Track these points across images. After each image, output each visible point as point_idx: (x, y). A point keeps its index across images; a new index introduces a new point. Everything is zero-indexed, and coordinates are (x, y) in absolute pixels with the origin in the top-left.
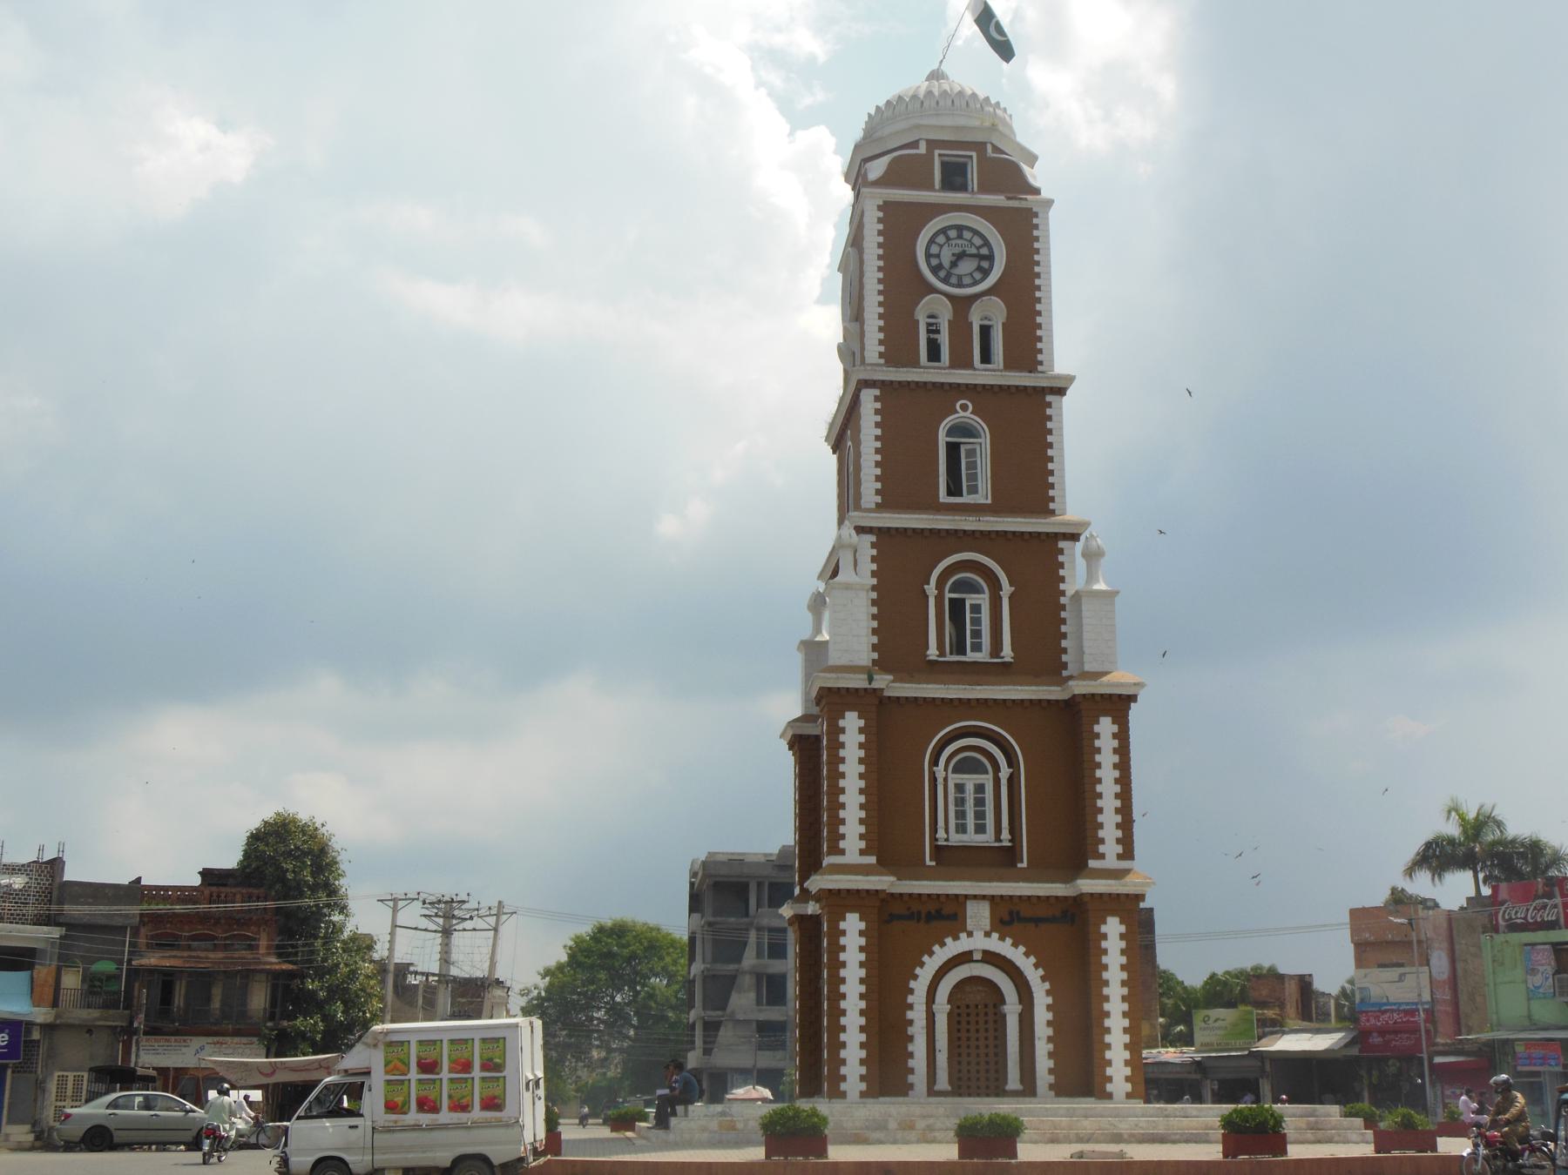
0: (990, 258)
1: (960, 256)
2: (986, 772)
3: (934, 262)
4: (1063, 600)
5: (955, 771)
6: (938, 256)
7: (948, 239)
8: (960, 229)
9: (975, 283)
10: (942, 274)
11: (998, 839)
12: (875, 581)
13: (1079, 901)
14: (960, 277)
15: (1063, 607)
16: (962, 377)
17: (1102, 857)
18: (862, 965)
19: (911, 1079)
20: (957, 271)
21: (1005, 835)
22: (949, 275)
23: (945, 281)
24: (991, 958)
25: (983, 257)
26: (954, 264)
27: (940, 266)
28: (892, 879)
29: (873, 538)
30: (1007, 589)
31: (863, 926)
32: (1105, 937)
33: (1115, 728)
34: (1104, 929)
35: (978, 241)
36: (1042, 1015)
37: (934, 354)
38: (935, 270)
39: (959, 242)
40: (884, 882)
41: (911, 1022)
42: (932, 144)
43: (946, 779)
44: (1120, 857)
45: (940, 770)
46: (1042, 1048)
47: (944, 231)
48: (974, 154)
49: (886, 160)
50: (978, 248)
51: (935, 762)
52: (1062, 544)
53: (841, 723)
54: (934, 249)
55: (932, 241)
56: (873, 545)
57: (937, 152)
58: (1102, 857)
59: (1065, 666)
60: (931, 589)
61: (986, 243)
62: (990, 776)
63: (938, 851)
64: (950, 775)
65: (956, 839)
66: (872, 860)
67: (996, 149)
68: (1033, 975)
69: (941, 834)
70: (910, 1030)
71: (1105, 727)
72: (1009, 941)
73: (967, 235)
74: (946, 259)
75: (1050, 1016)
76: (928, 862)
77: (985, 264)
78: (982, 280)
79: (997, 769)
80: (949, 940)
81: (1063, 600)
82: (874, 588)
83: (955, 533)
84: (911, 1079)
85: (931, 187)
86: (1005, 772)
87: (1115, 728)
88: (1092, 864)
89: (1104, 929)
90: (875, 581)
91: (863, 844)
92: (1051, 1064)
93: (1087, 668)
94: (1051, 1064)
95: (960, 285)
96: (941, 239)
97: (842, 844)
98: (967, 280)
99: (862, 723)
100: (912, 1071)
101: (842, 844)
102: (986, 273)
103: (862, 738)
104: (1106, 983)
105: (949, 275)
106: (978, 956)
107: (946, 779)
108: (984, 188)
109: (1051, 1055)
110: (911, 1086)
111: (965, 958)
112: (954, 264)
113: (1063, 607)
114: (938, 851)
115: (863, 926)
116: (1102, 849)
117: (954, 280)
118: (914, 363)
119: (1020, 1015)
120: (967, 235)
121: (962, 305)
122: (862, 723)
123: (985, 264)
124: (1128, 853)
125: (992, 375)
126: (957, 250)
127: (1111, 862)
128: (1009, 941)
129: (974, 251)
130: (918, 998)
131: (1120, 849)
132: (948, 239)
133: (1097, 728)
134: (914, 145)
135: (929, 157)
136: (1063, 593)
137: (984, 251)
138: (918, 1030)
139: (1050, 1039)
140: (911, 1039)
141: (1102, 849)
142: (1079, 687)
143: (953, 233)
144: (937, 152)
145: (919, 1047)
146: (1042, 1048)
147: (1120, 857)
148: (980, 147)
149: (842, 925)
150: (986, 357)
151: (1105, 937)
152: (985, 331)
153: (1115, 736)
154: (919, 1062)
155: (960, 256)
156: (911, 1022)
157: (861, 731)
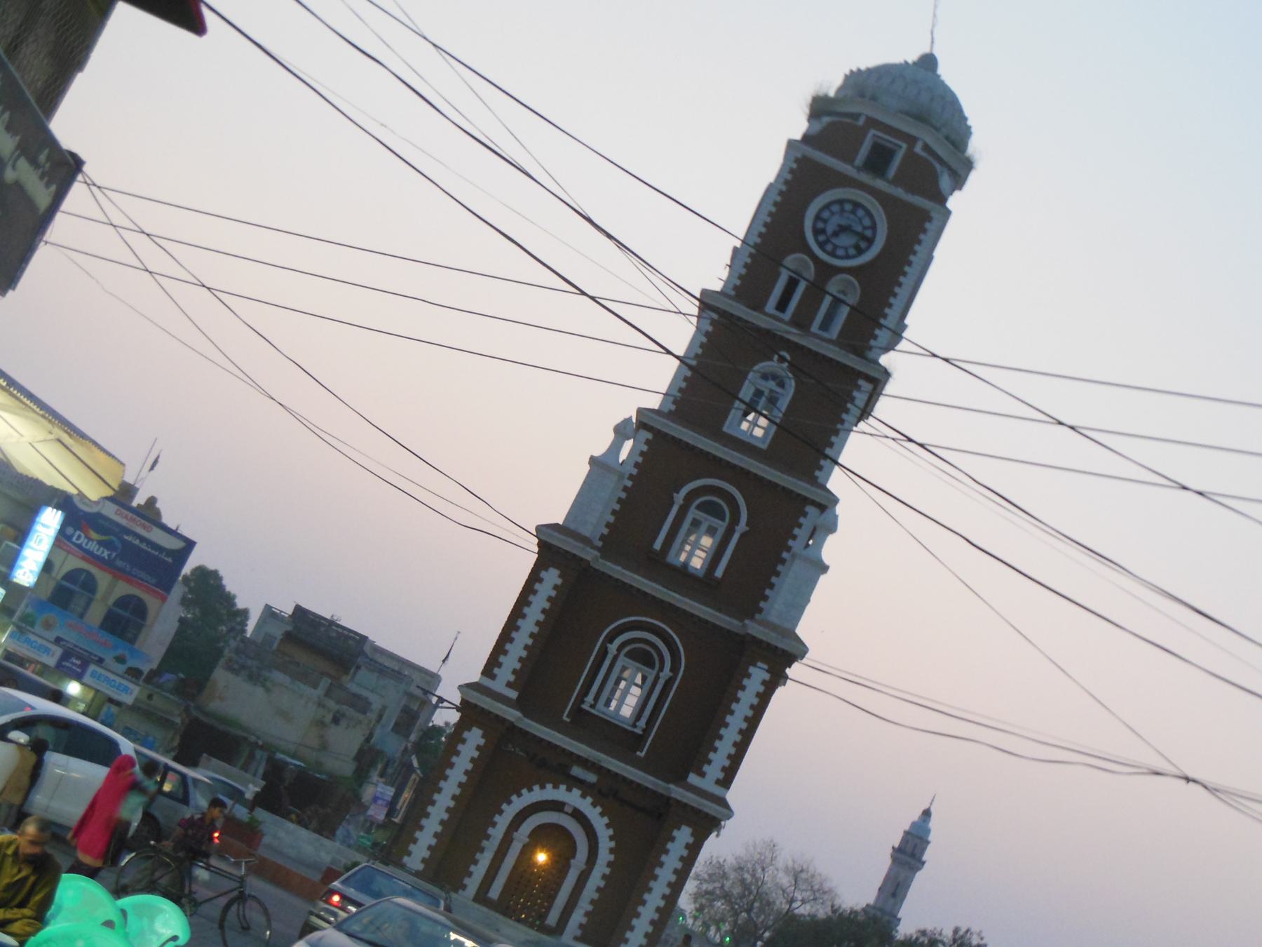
0: (870, 241)
1: (843, 229)
2: (651, 666)
3: (820, 225)
4: (785, 555)
5: (628, 655)
6: (825, 221)
7: (843, 210)
8: (857, 205)
9: (848, 257)
10: (822, 238)
11: (634, 726)
12: (635, 471)
13: (667, 801)
14: (835, 247)
15: (783, 561)
16: (794, 335)
17: (702, 775)
18: (466, 772)
19: (467, 881)
20: (834, 240)
21: (642, 723)
22: (827, 241)
23: (822, 245)
24: (578, 815)
25: (864, 238)
26: (836, 234)
27: (823, 231)
28: (518, 714)
29: (649, 436)
30: (742, 527)
31: (482, 742)
32: (673, 839)
33: (767, 676)
34: (675, 833)
35: (867, 222)
36: (596, 880)
37: (782, 305)
38: (817, 232)
39: (852, 216)
40: (512, 715)
41: (488, 837)
42: (872, 123)
43: (615, 658)
44: (718, 782)
45: (613, 648)
46: (584, 905)
47: (841, 202)
48: (904, 146)
49: (826, 120)
50: (865, 228)
51: (610, 639)
52: (810, 509)
53: (543, 574)
54: (826, 215)
55: (827, 206)
56: (647, 442)
57: (873, 132)
58: (702, 775)
59: (760, 610)
60: (679, 498)
61: (874, 227)
62: (655, 672)
63: (578, 712)
64: (622, 656)
65: (600, 710)
66: (513, 694)
67: (926, 148)
68: (605, 843)
69: (590, 699)
70: (485, 843)
71: (758, 675)
72: (599, 809)
73: (860, 213)
74: (830, 228)
75: (602, 884)
76: (565, 718)
77: (863, 245)
78: (854, 257)
79: (661, 669)
80: (549, 786)
81: (785, 555)
82: (631, 477)
83: (719, 461)
84: (467, 881)
85: (849, 160)
86: (666, 673)
87: (767, 676)
88: (693, 779)
89: (675, 833)
90: (635, 471)
91: (512, 678)
92: (584, 920)
93: (773, 617)
94: (584, 920)
95: (832, 254)
96: (836, 208)
97: (496, 671)
98: (840, 252)
99: (559, 581)
100: (470, 874)
101: (496, 671)
102: (860, 251)
103: (553, 593)
104: (655, 878)
105: (827, 241)
106: (567, 809)
107: (615, 658)
108: (896, 182)
109: (587, 914)
110: (464, 887)
111: (557, 806)
112: (836, 234)
113: (783, 561)
114: (578, 712)
115: (482, 742)
116: (706, 768)
117: (829, 247)
118: (758, 306)
119: (582, 872)
120: (860, 213)
121: (827, 272)
122: (559, 581)
123: (863, 245)
124: (727, 780)
125: (823, 341)
126: (844, 222)
127: (707, 783)
128: (599, 809)
129: (859, 229)
130: (503, 822)
131: (721, 775)
132: (843, 210)
133: (752, 670)
134: (856, 116)
135: (863, 132)
136: (789, 549)
137: (868, 233)
138: (491, 846)
139: (592, 902)
140: (482, 850)
141: (706, 768)
142: (754, 629)
143: (848, 207)
144: (873, 132)
145: (485, 860)
146: (584, 905)
147: (718, 782)
148: (911, 140)
149: (466, 735)
150: (825, 326)
151: (673, 839)
152: (837, 302)
153: (764, 683)
154: (479, 870)
155: (843, 229)
156: (488, 837)
157: (556, 587)
